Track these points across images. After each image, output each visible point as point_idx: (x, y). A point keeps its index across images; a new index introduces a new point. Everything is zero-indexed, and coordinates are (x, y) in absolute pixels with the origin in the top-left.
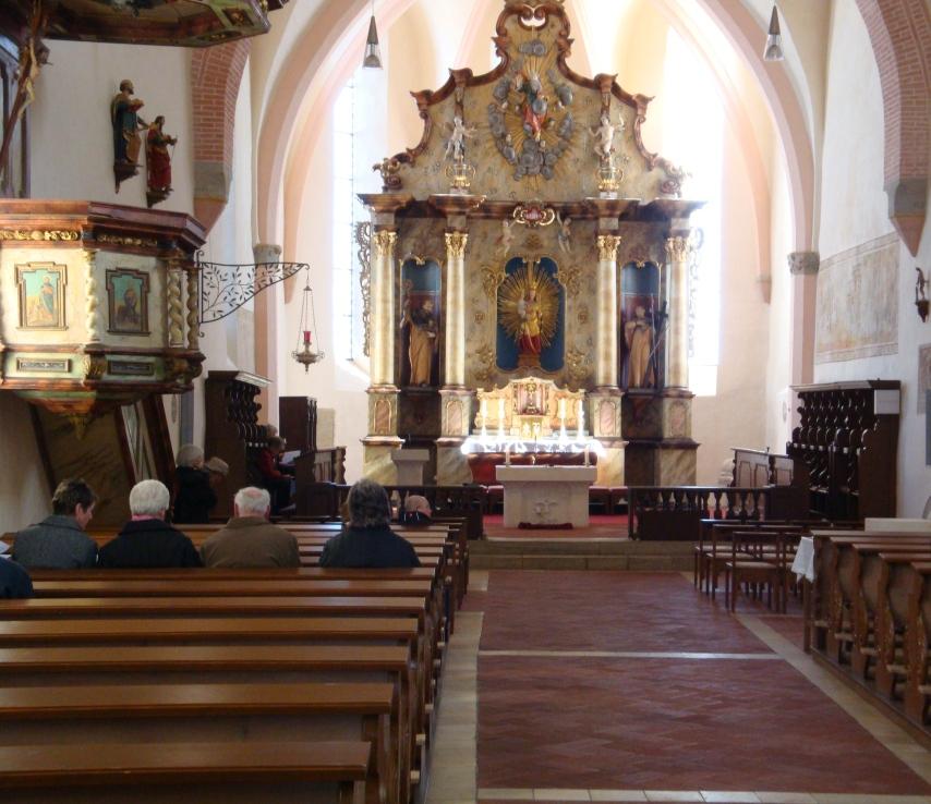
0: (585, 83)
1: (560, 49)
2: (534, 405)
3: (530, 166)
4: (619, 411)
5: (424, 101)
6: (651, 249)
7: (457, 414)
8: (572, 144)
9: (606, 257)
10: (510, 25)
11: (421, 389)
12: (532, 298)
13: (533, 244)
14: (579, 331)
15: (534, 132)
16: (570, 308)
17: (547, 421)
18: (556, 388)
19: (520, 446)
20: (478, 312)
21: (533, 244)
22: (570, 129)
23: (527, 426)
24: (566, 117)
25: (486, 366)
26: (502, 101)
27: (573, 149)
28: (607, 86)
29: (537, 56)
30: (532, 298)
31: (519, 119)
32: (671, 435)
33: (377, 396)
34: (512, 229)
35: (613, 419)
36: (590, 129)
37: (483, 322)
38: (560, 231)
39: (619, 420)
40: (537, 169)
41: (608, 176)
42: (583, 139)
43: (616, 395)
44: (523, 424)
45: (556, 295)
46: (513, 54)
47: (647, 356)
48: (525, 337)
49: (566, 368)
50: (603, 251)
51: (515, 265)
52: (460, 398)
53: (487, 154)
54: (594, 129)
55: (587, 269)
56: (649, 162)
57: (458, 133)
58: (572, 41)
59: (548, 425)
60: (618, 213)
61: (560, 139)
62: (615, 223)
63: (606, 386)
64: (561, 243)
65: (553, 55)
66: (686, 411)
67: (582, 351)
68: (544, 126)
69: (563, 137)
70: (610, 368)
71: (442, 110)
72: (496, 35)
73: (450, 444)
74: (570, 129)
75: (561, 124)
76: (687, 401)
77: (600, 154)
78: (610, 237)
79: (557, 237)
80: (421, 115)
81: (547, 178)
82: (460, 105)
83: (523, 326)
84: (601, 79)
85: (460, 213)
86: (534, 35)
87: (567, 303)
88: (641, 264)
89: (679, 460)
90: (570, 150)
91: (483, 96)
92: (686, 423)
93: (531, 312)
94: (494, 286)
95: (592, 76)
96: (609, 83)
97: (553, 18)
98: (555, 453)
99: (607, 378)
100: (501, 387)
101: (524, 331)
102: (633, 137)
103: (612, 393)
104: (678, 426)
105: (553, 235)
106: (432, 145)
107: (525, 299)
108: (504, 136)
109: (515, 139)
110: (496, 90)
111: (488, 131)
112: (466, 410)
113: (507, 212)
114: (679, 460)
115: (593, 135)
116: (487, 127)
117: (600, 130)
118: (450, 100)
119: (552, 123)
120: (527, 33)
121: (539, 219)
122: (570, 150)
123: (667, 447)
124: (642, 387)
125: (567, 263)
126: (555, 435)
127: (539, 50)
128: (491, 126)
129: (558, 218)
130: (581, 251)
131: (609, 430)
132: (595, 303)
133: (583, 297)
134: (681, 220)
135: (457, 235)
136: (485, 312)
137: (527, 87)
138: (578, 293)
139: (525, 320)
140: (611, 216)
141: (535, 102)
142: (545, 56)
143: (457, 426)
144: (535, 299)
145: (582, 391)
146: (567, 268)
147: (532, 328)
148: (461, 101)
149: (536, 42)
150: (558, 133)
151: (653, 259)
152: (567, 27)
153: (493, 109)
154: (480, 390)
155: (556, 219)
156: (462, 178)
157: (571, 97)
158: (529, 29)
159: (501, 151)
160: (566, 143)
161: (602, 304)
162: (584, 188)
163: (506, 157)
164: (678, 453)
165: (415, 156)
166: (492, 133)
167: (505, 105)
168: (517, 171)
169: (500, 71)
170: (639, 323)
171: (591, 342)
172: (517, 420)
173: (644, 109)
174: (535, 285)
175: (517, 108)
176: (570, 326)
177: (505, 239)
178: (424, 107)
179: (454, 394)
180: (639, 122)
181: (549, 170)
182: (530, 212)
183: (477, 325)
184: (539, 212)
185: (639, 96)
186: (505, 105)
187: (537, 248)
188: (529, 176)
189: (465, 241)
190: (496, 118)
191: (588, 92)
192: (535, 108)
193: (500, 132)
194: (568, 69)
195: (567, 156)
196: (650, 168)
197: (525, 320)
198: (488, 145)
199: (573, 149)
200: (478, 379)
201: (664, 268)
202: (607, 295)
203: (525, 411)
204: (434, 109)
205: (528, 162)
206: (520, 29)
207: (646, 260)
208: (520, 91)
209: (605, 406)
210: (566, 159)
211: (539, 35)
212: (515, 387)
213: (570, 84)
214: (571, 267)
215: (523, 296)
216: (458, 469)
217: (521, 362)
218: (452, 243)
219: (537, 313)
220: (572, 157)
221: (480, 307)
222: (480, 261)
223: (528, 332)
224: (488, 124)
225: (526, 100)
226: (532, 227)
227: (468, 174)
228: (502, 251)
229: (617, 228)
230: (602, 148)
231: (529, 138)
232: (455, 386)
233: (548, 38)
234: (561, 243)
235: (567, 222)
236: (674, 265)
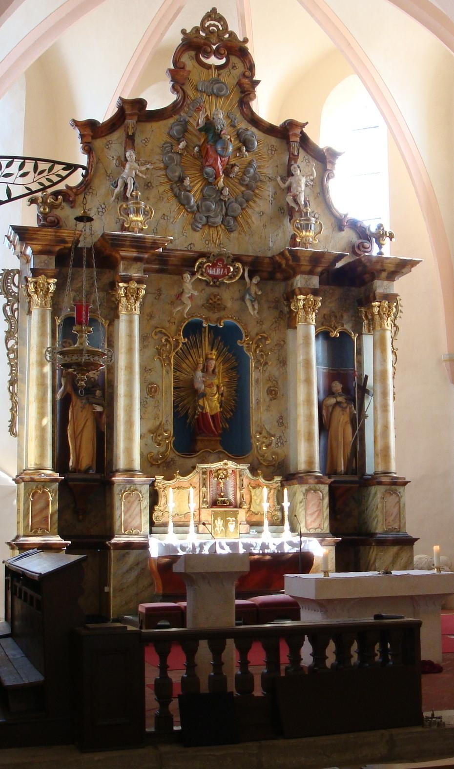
0: (269, 130)
1: (243, 92)
2: (226, 495)
3: (212, 214)
4: (326, 501)
5: (88, 132)
6: (345, 317)
7: (135, 508)
8: (256, 195)
9: (306, 320)
10: (187, 59)
11: (86, 476)
12: (211, 369)
13: (214, 304)
14: (268, 409)
15: (217, 177)
16: (257, 381)
17: (242, 515)
18: (250, 475)
19: (222, 548)
20: (152, 383)
21: (214, 304)
22: (254, 178)
23: (219, 522)
24: (250, 164)
25: (162, 449)
26: (179, 141)
27: (257, 200)
28: (295, 135)
29: (218, 96)
30: (211, 369)
31: (198, 163)
32: (182, 571)
33: (33, 486)
34: (193, 284)
35: (320, 511)
36: (279, 179)
37: (158, 396)
38: (248, 290)
39: (326, 512)
40: (219, 220)
41: (307, 227)
42: (268, 191)
43: (323, 483)
44: (215, 518)
45: (233, 368)
46: (191, 93)
47: (350, 439)
48: (204, 415)
49: (254, 451)
50: (301, 314)
51: (193, 329)
52: (138, 487)
53: (160, 198)
54: (284, 180)
55: (275, 337)
56: (340, 224)
57: (131, 169)
58: (258, 82)
59: (244, 519)
60: (319, 269)
61: (243, 189)
62: (315, 281)
63: (309, 472)
64: (248, 304)
65: (235, 97)
66: (399, 502)
67: (272, 432)
68: (227, 172)
69: (247, 186)
70: (314, 451)
71: (108, 145)
72: (172, 67)
73: (129, 546)
74: (254, 178)
75: (245, 172)
76: (401, 489)
77: (292, 204)
78: (311, 297)
79: (243, 299)
80: (84, 148)
81: (230, 230)
82: (130, 140)
83: (201, 402)
84: (290, 125)
85: (137, 260)
86: (214, 74)
87: (254, 375)
88: (335, 334)
89: (396, 556)
90: (255, 202)
91: (157, 133)
92: (400, 515)
93: (210, 386)
94: (170, 353)
95: (277, 122)
96: (298, 131)
97: (234, 59)
98: (264, 554)
99: (310, 462)
100: (184, 474)
101: (203, 408)
102: (321, 191)
103: (319, 481)
104: (392, 518)
105: (237, 295)
106: (96, 183)
107: (203, 371)
108: (181, 180)
109: (194, 186)
110: (171, 128)
111: (163, 172)
112: (146, 503)
113: (188, 263)
114: (396, 556)
115: (283, 186)
116: (160, 169)
117: (290, 179)
118: (117, 137)
119: (236, 169)
120: (205, 71)
121: (224, 276)
122: (255, 202)
123: (382, 543)
124: (346, 473)
125: (253, 329)
126: (253, 531)
127: (220, 90)
128: (166, 168)
129: (246, 275)
130: (269, 317)
131: (316, 525)
132: (285, 376)
133: (273, 369)
134: (386, 283)
135: (134, 285)
136: (160, 384)
137: (209, 127)
138: (266, 363)
139: (204, 395)
140: (311, 273)
141: (220, 141)
142: (227, 97)
143: (135, 523)
144: (214, 371)
145: (278, 479)
146: (253, 333)
147: (212, 405)
148: (134, 134)
149: (217, 81)
150: (241, 181)
151: (348, 327)
152: (251, 68)
153: (168, 148)
154: (159, 478)
155: (243, 277)
156: (140, 218)
157: (256, 143)
158: (209, 67)
159: (177, 196)
160: (250, 192)
161: (301, 375)
162: (271, 245)
163: (183, 203)
164: (395, 549)
165: (76, 194)
166: (166, 175)
167: (182, 145)
168: (196, 220)
169: (173, 110)
170: (340, 399)
171: (283, 421)
172: (207, 514)
173: (333, 164)
174: (214, 354)
175: (196, 149)
176: (258, 403)
177: (186, 296)
178: (89, 139)
179: (131, 482)
180: (328, 178)
181: (232, 223)
182: (214, 266)
183: (149, 400)
184: (225, 267)
185: (329, 150)
186: (182, 145)
187: (219, 310)
188: (210, 227)
189: (143, 292)
190: (171, 159)
191: (273, 141)
192: (219, 149)
193: (177, 174)
194: (252, 113)
195: (251, 207)
196: (341, 229)
197: (204, 395)
198: (162, 189)
199: (257, 200)
200: (152, 465)
201: (360, 338)
202: (307, 364)
203: (214, 504)
204: (99, 143)
205: (208, 210)
206: (196, 65)
207: (339, 329)
208: (200, 130)
209: (311, 495)
210: (250, 211)
211: (219, 75)
212: (204, 473)
213: (254, 130)
214: (257, 334)
215: (201, 366)
216: (138, 577)
217: (200, 445)
218: (126, 295)
219: (218, 387)
220: (257, 209)
221: (153, 377)
222: (154, 322)
223: (208, 410)
224: (162, 165)
225: (206, 141)
226: (215, 286)
227: (146, 213)
228: (183, 309)
229: (317, 286)
230: (296, 201)
231: (210, 184)
232: (130, 471)
233: (230, 79)
234: (248, 304)
235: (255, 280)
236: (378, 334)
